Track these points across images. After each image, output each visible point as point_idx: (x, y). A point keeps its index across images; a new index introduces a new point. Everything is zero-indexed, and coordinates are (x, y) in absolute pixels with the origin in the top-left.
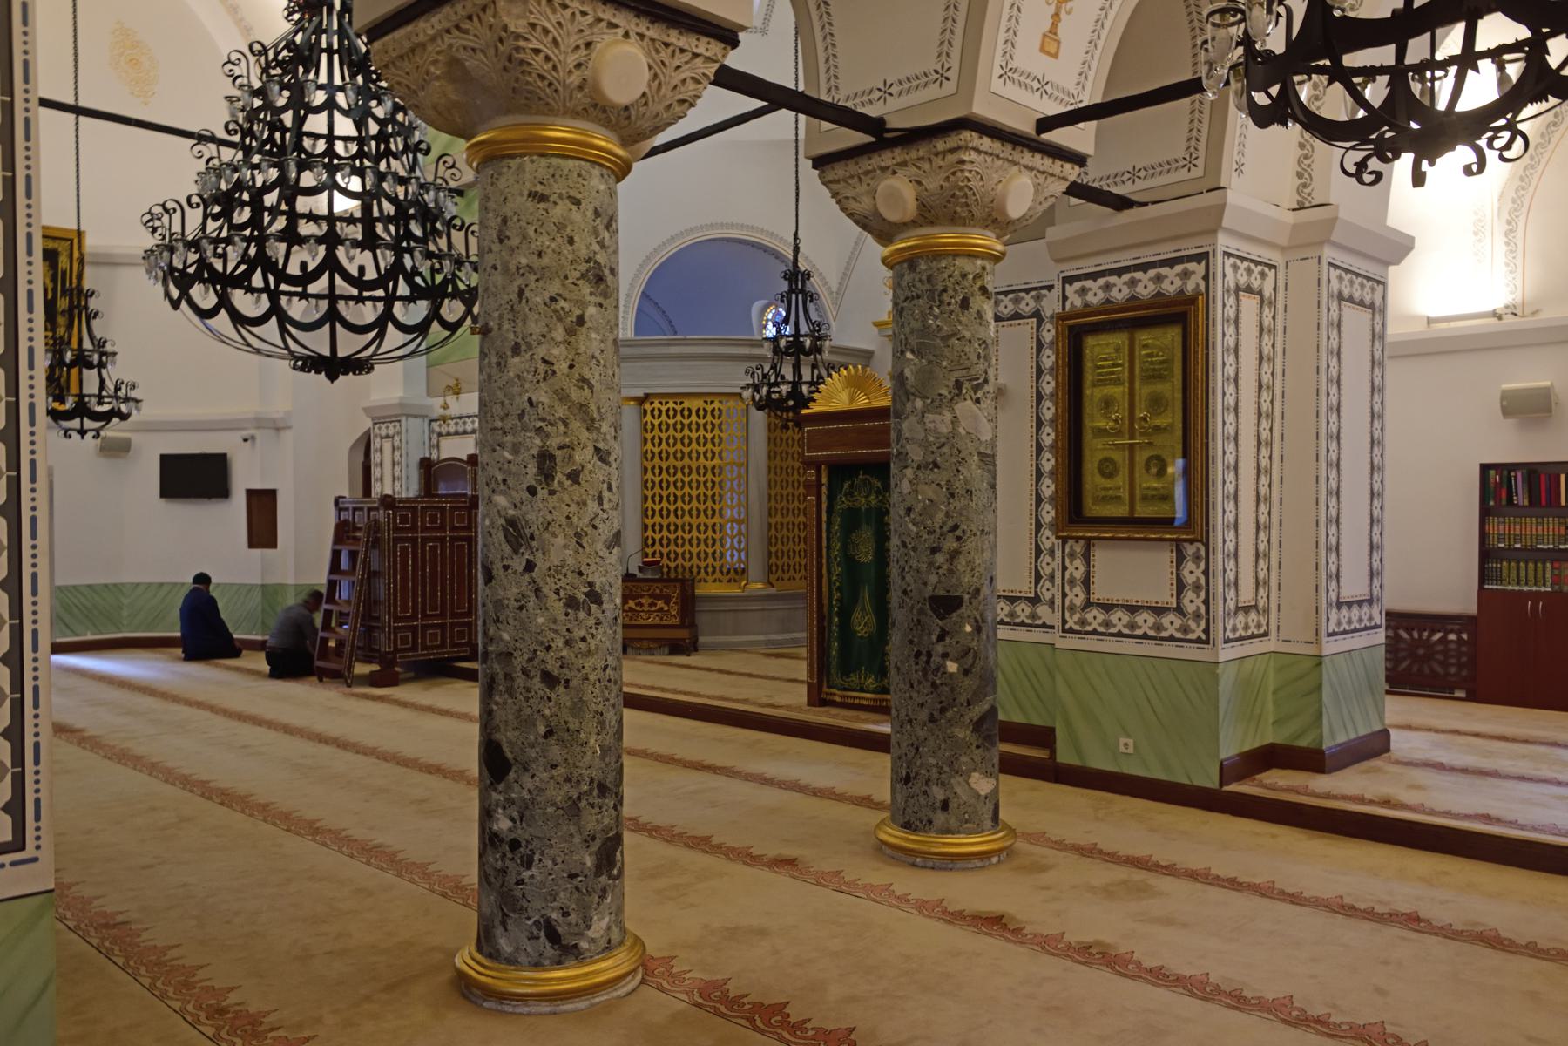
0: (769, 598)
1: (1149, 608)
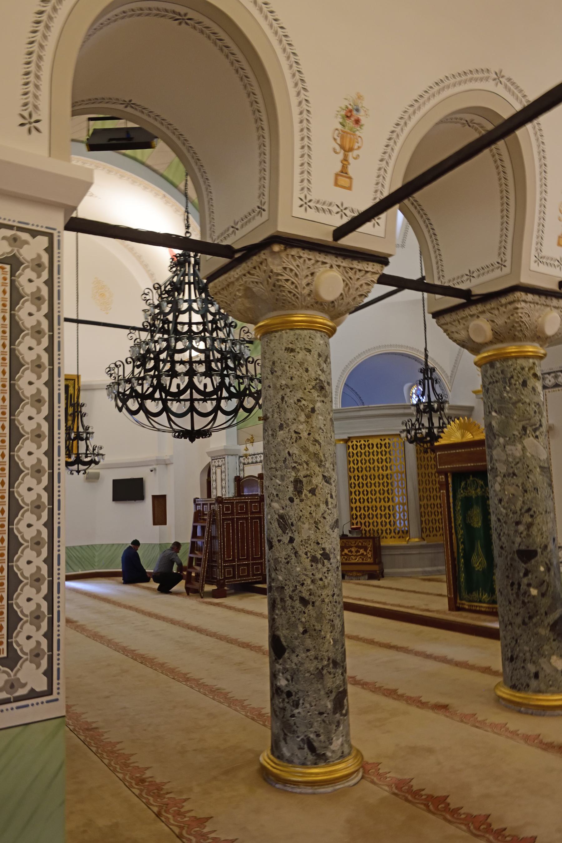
0: (422, 547)
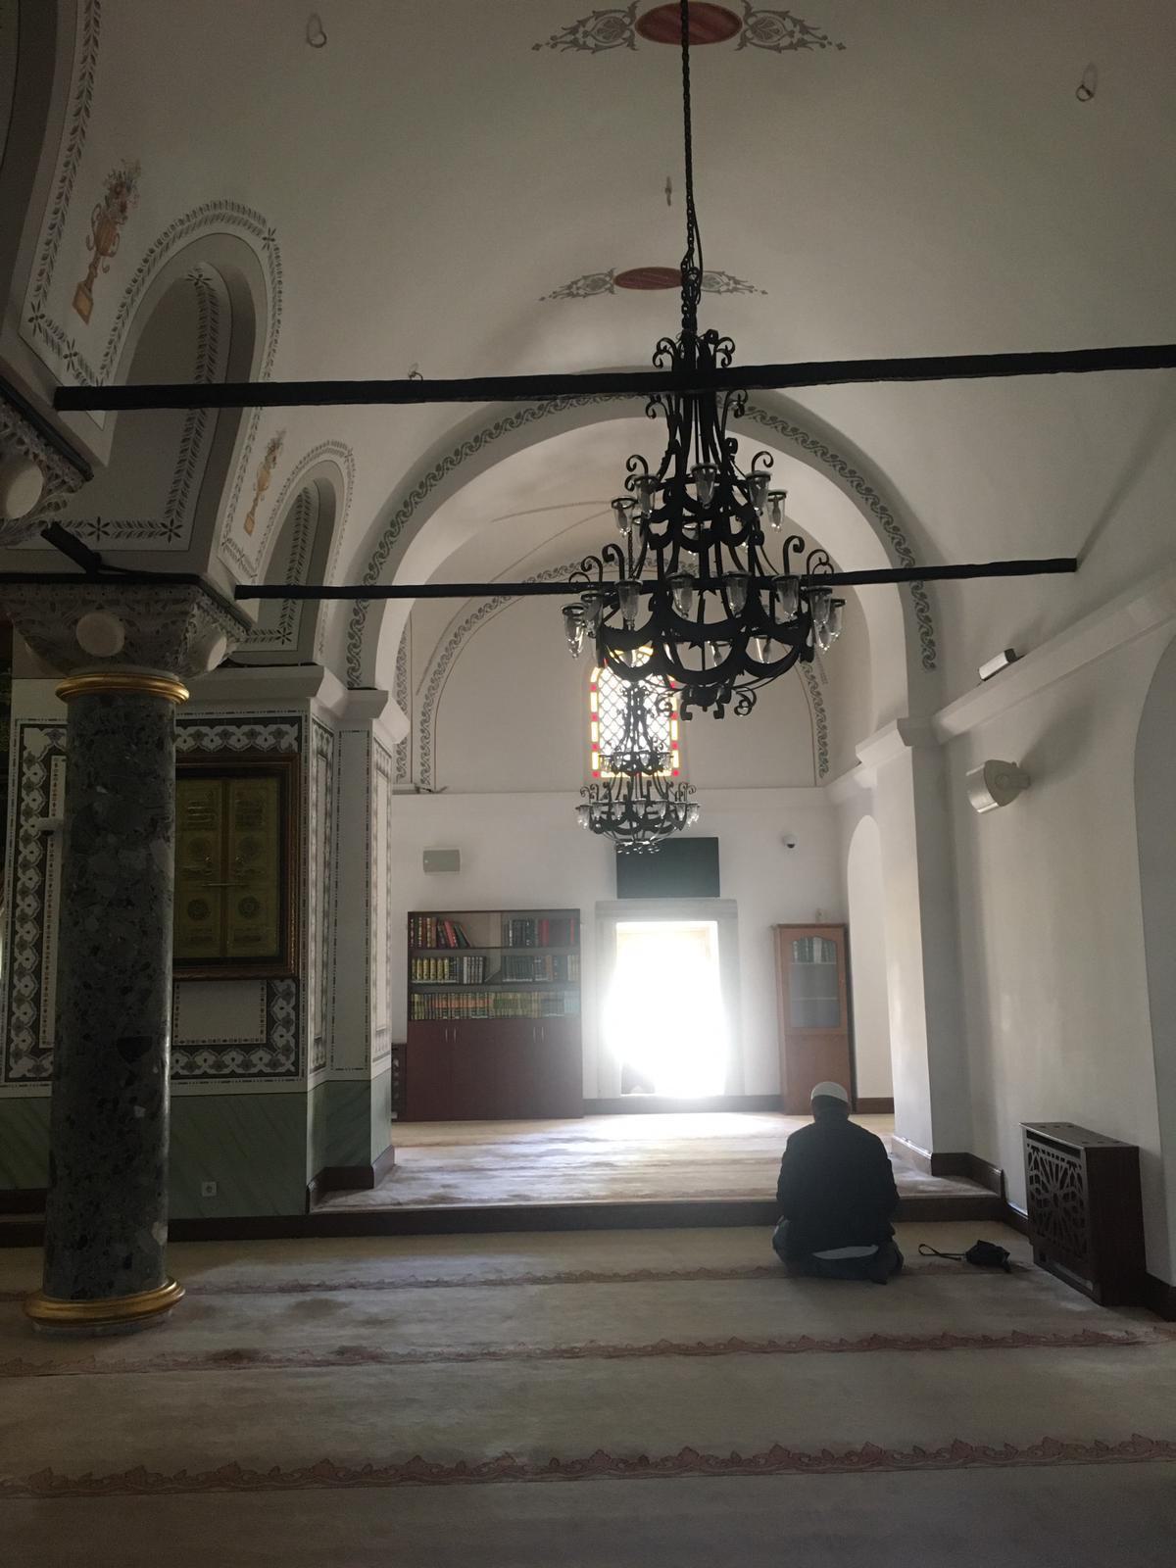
1: (209, 1047)
